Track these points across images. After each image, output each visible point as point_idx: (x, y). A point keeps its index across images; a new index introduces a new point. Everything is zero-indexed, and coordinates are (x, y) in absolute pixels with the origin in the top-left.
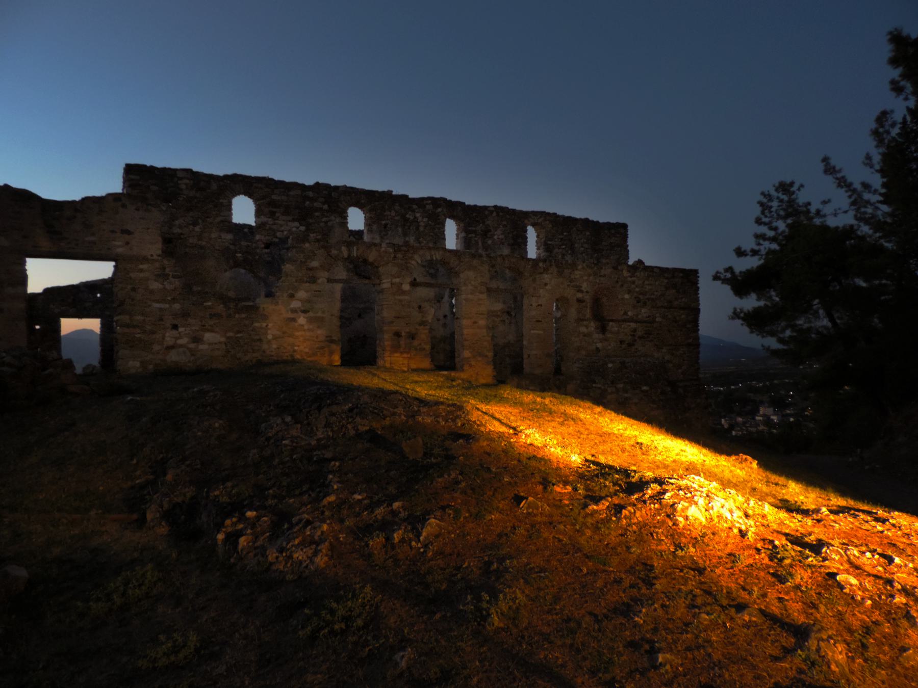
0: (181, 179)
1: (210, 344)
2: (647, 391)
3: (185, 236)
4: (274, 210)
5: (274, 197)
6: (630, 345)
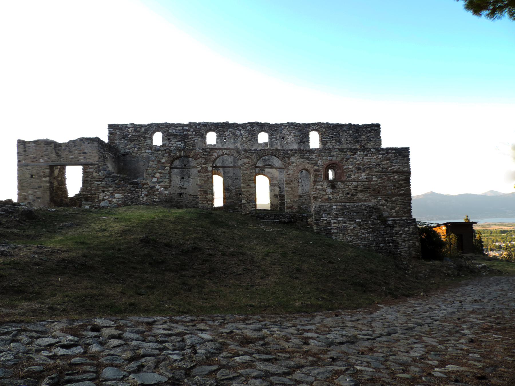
0: (129, 128)
1: (117, 198)
2: (360, 222)
5: (170, 131)
6: (353, 195)
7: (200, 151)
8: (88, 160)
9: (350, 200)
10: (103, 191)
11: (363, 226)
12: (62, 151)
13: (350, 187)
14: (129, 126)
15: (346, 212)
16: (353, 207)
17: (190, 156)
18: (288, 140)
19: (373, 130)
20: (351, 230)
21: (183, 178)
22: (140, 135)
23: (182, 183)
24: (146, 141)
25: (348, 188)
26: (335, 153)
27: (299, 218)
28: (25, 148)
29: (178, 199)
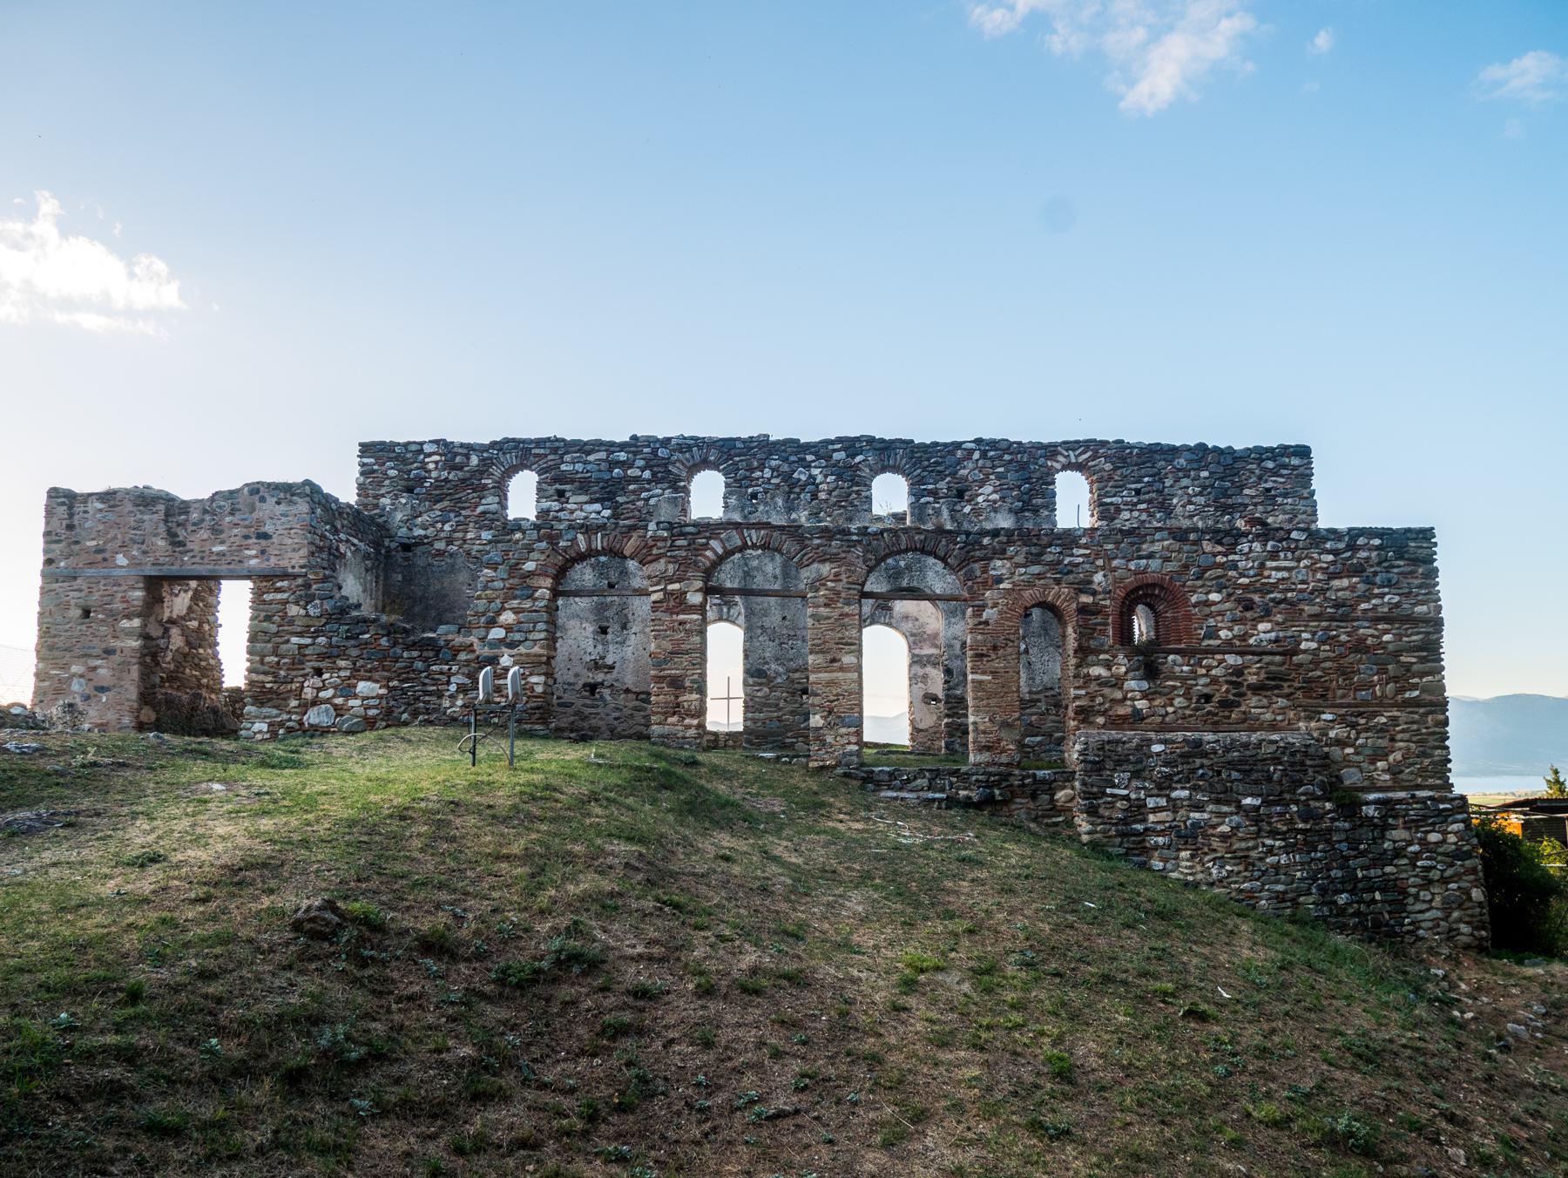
0: (430, 455)
1: (364, 699)
2: (1257, 808)
4: (563, 487)
5: (563, 467)
6: (1226, 704)
7: (660, 533)
8: (273, 560)
9: (1216, 723)
11: (1270, 824)
12: (191, 528)
13: (1213, 672)
14: (427, 448)
15: (1202, 766)
16: (1227, 750)
17: (627, 553)
18: (980, 499)
19: (1285, 466)
20: (1224, 837)
21: (604, 631)
22: (463, 480)
23: (600, 647)
24: (483, 501)
25: (1206, 675)
26: (1157, 547)
27: (1024, 785)
28: (71, 515)
29: (584, 705)
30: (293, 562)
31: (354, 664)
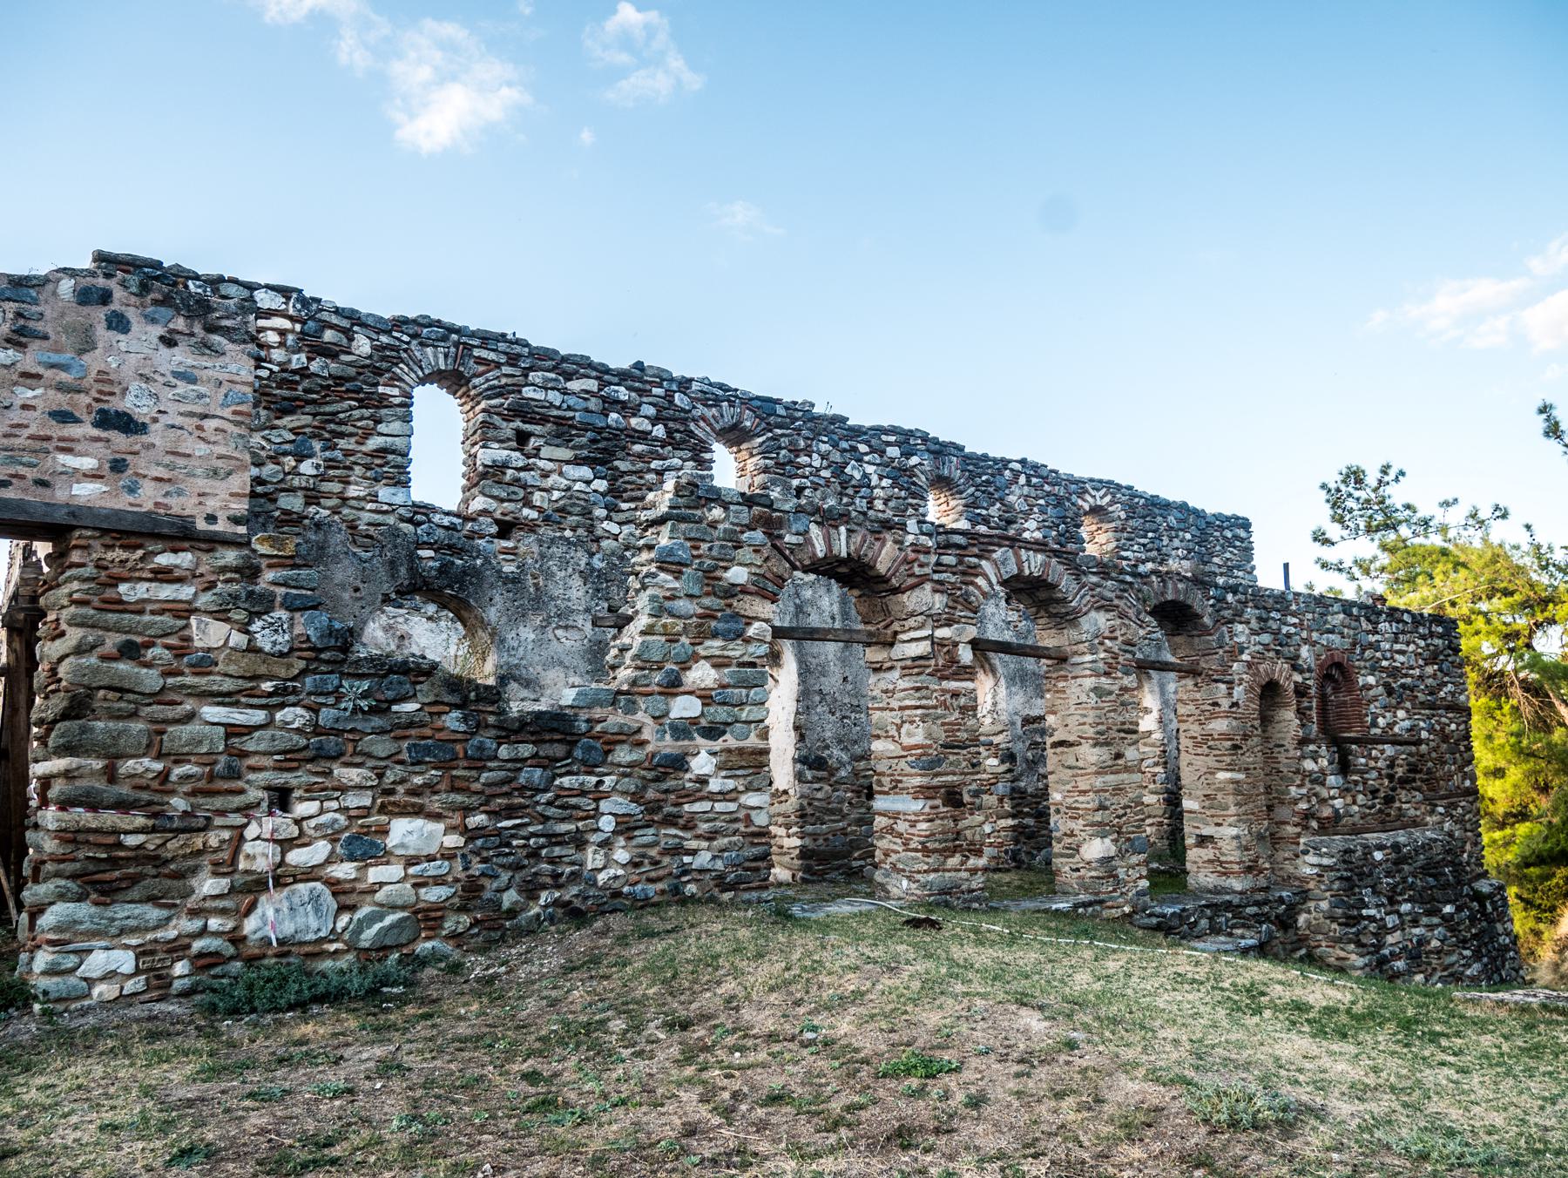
0: (269, 314)
1: (411, 861)
3: (270, 488)
5: (528, 392)
7: (923, 539)
8: (148, 497)
10: (281, 799)
14: (265, 300)
22: (340, 380)
24: (382, 428)
30: (212, 505)
31: (380, 776)
